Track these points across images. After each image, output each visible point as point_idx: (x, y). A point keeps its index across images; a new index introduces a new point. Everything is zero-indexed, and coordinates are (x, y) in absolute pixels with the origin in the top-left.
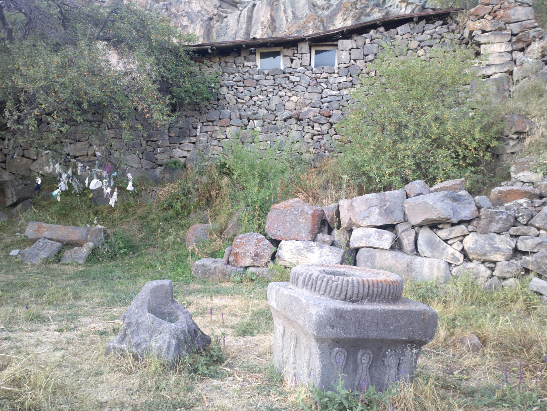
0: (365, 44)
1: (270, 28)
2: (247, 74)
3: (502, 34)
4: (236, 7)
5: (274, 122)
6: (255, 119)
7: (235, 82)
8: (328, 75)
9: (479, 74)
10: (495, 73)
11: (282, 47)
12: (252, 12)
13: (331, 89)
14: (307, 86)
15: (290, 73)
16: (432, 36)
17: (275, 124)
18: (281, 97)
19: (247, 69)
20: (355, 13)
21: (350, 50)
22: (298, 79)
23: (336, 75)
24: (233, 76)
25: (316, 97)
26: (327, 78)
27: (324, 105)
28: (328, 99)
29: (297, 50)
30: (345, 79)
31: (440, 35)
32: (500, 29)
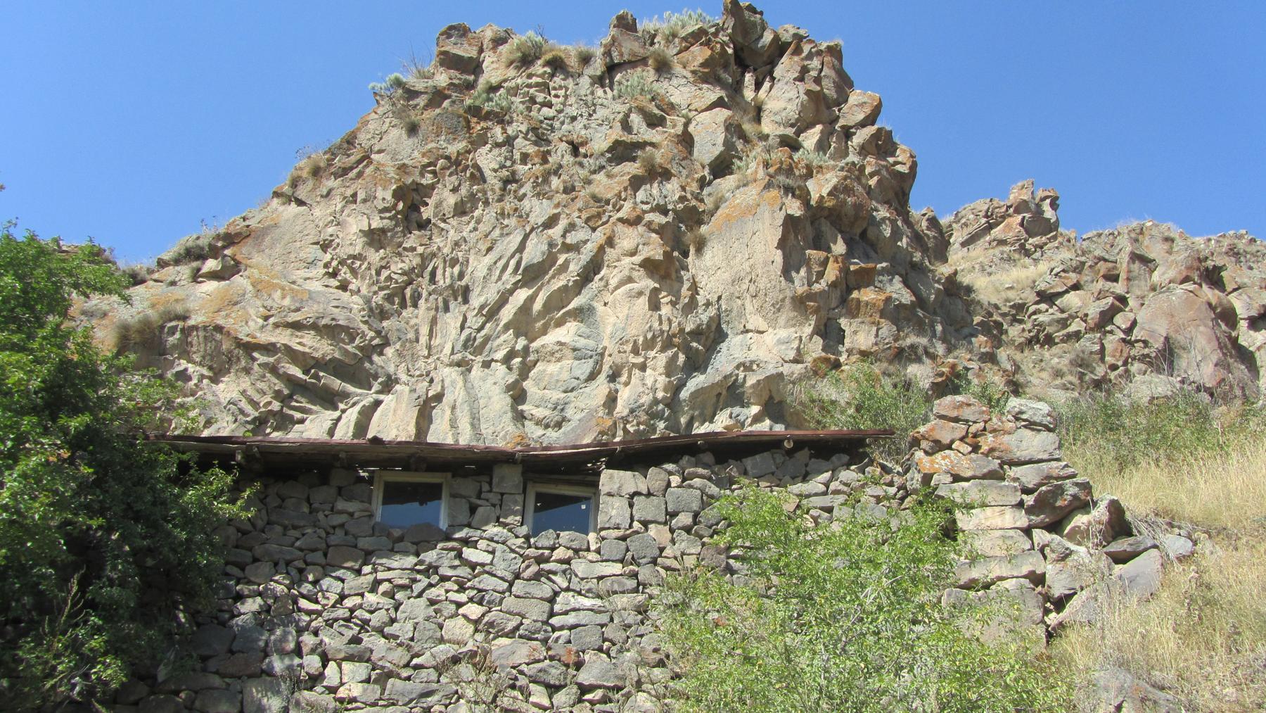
0: (669, 485)
2: (340, 533)
3: (1001, 488)
5: (405, 673)
6: (345, 659)
7: (301, 550)
8: (570, 553)
9: (964, 579)
10: (1001, 579)
11: (449, 475)
13: (579, 593)
14: (509, 577)
17: (409, 678)
18: (432, 602)
19: (341, 519)
21: (632, 496)
22: (487, 558)
23: (592, 556)
24: (296, 533)
25: (536, 611)
26: (567, 561)
27: (557, 634)
28: (571, 619)
29: (490, 484)
30: (617, 568)
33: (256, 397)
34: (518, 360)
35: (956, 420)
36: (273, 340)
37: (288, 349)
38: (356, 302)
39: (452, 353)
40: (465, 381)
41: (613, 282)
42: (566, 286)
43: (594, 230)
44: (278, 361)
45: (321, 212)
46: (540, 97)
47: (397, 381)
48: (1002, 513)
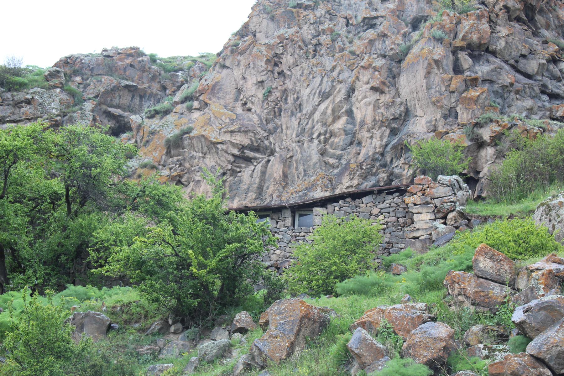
0: (334, 210)
1: (281, 184)
4: (251, 162)
8: (305, 234)
10: (422, 235)
12: (266, 168)
15: (275, 232)
16: (390, 204)
20: (360, 174)
22: (281, 237)
26: (304, 236)
31: (396, 204)
32: (427, 203)
33: (222, 164)
34: (322, 137)
35: (420, 184)
36: (224, 139)
37: (231, 142)
38: (255, 118)
39: (297, 137)
40: (301, 150)
41: (360, 98)
42: (341, 101)
43: (352, 70)
44: (228, 148)
45: (237, 73)
47: (275, 151)
48: (427, 215)
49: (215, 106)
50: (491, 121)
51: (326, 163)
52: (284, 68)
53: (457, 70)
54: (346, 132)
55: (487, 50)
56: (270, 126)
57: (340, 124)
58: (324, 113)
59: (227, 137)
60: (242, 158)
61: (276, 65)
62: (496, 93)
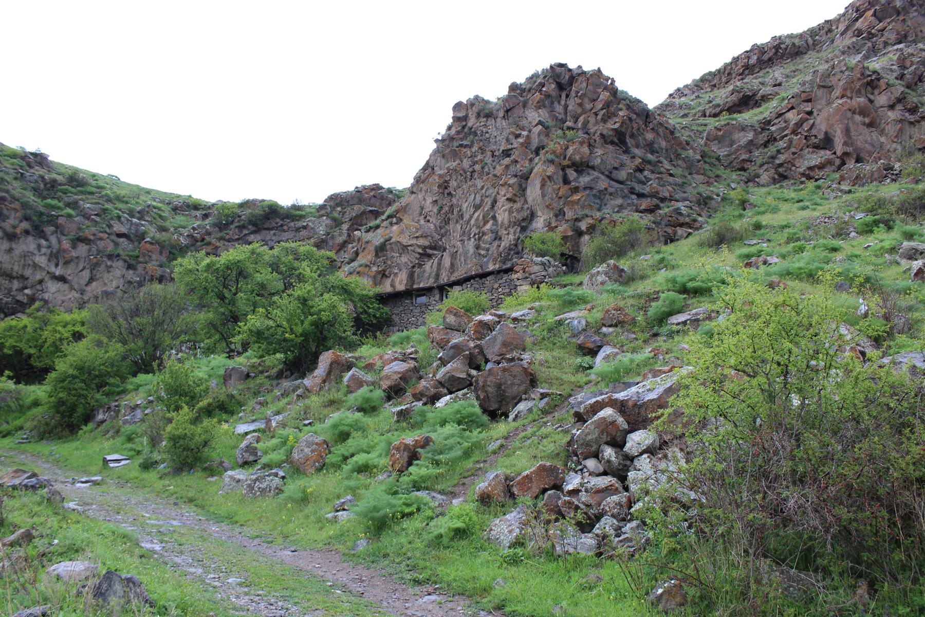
45: (420, 196)
46: (484, 130)
49: (406, 221)
50: (587, 216)
51: (480, 254)
52: (451, 190)
53: (566, 181)
54: (492, 231)
55: (588, 166)
56: (443, 231)
57: (488, 226)
58: (477, 219)
59: (414, 242)
60: (425, 255)
61: (446, 188)
62: (595, 196)
